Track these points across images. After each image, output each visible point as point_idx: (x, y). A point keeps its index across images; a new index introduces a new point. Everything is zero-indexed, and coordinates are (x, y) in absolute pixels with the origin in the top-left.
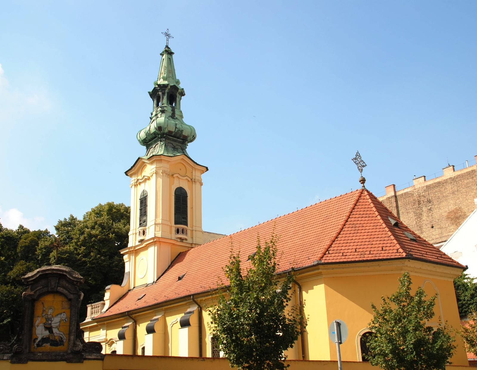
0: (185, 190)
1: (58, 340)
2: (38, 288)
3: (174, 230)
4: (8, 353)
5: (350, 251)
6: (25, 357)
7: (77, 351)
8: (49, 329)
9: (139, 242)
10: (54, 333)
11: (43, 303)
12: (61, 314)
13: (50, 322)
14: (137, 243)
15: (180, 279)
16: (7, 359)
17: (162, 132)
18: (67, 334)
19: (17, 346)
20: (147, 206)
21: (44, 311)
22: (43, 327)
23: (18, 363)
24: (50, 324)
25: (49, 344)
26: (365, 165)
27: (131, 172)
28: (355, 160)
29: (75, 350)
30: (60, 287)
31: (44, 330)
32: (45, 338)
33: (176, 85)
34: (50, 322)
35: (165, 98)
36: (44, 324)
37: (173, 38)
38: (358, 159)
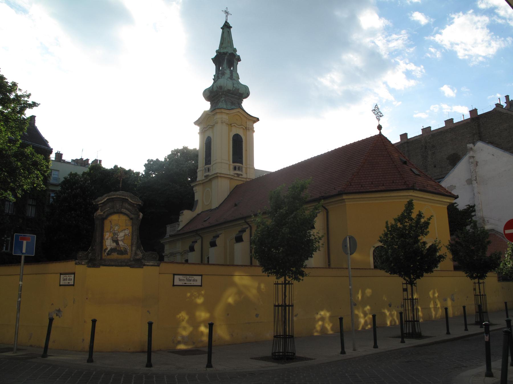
0: (241, 136)
1: (123, 250)
2: (106, 210)
3: (232, 167)
4: (85, 260)
5: (367, 183)
6: (98, 263)
7: (138, 259)
8: (116, 241)
9: (205, 177)
10: (120, 244)
11: (110, 221)
12: (125, 230)
13: (116, 236)
14: (204, 178)
15: (236, 205)
16: (85, 264)
18: (130, 246)
19: (92, 254)
21: (111, 227)
22: (111, 240)
23: (93, 267)
24: (117, 238)
25: (116, 253)
26: (382, 115)
28: (374, 111)
29: (136, 258)
30: (123, 208)
31: (112, 242)
32: (113, 249)
33: (234, 52)
34: (116, 236)
36: (112, 237)
37: (231, 15)
38: (377, 110)
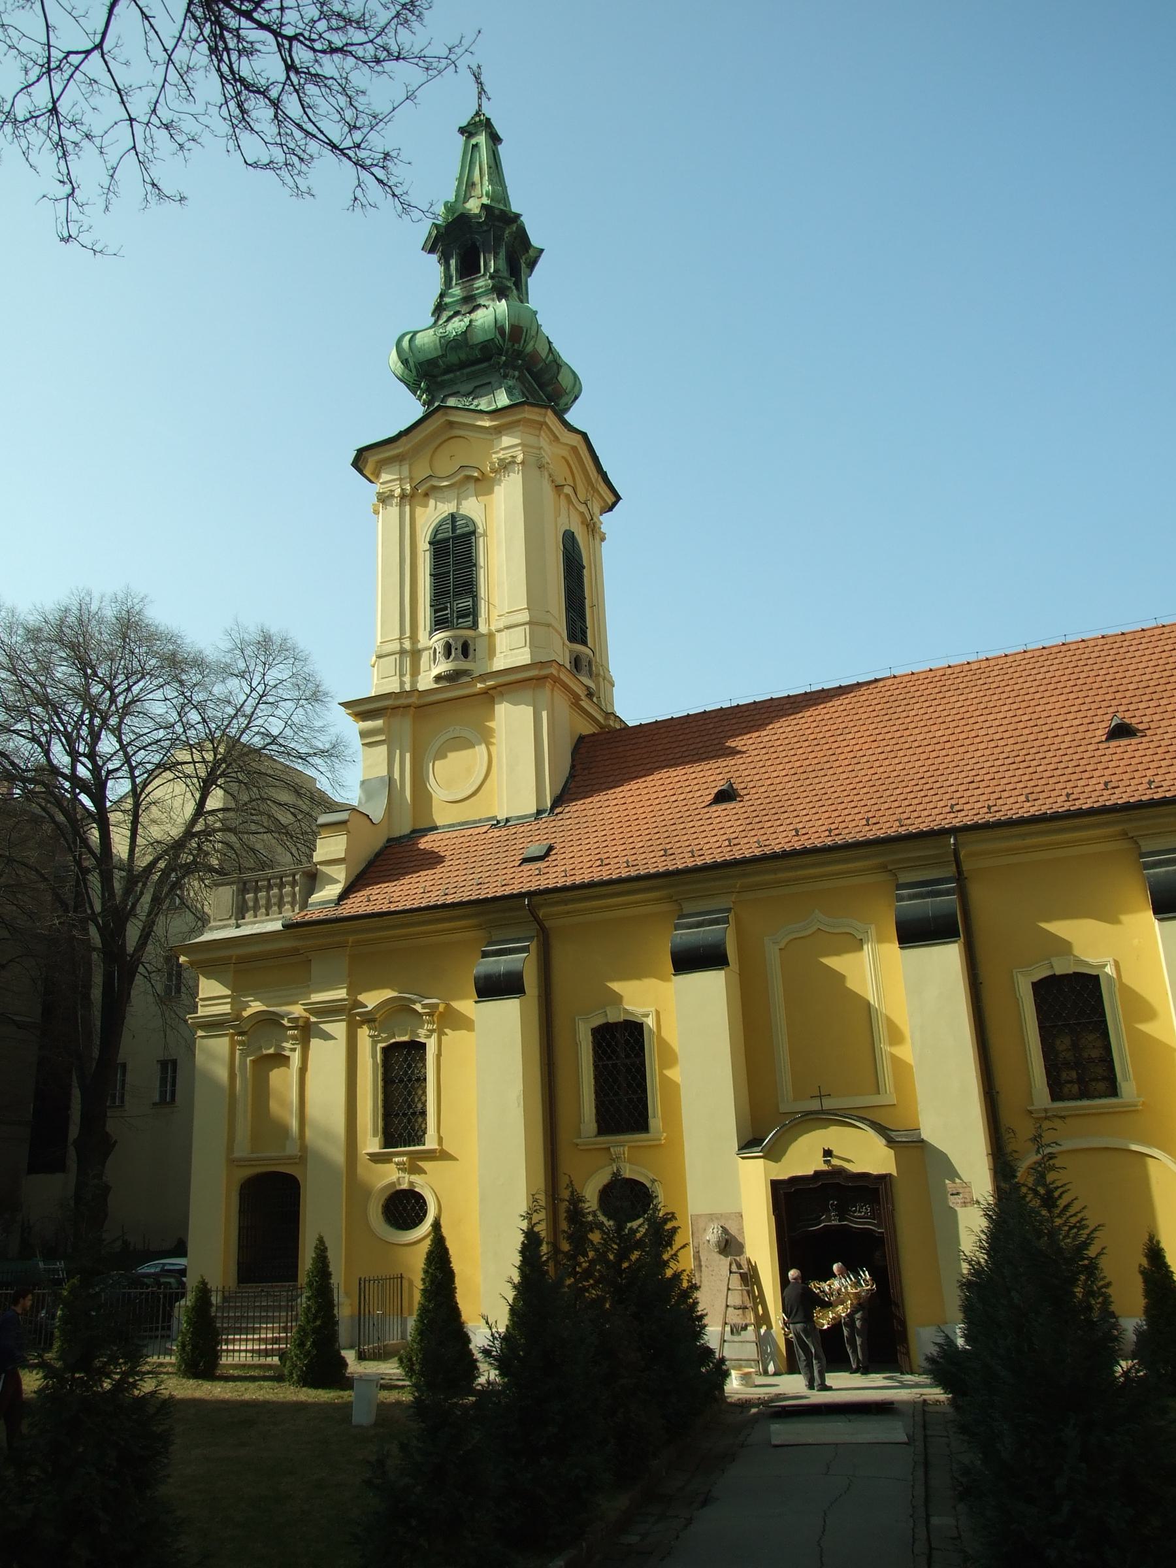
17: (516, 346)
27: (394, 449)
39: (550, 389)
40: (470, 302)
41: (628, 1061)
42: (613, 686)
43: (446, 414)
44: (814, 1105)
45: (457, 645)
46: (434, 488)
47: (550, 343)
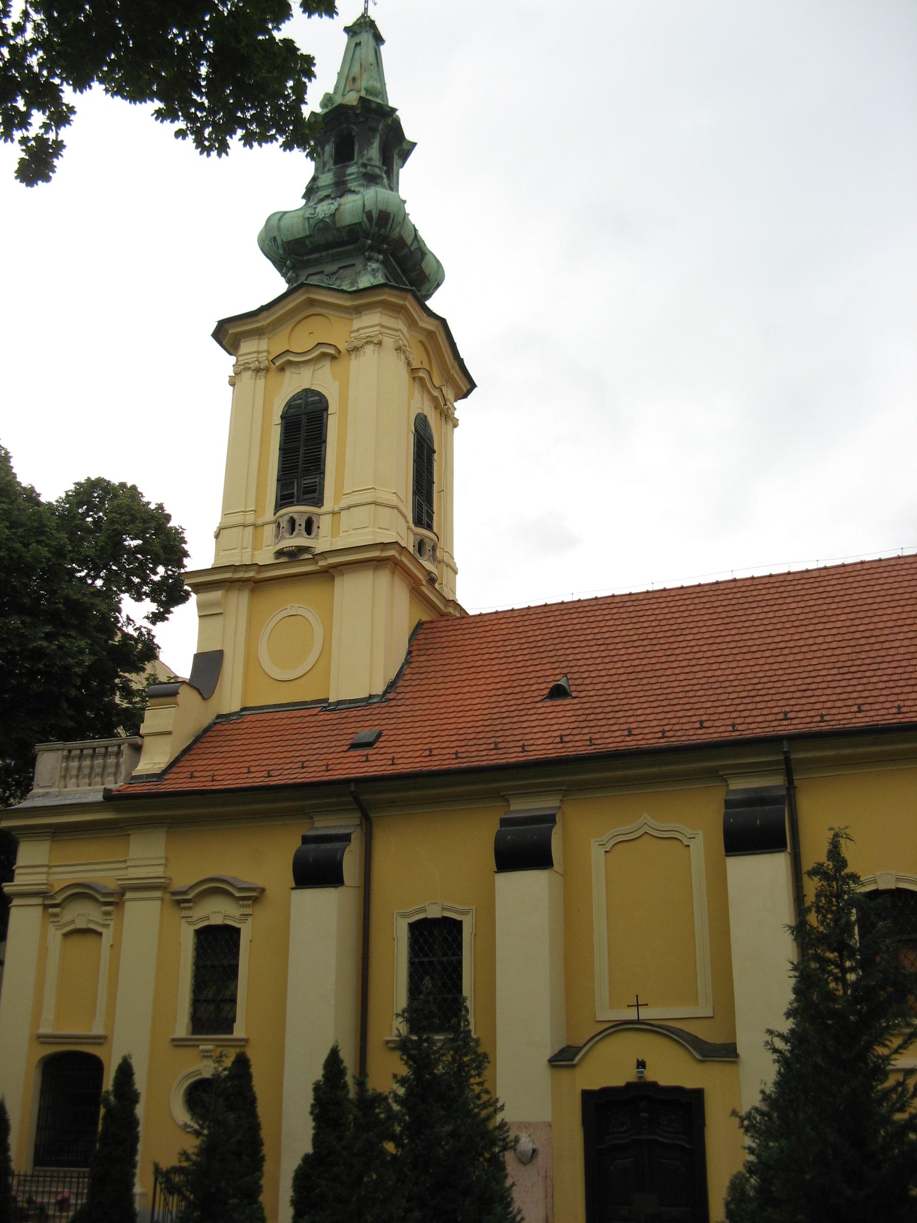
17: (382, 231)
20: (325, 442)
35: (375, 144)
39: (413, 275)
40: (341, 188)
41: (445, 959)
42: (456, 573)
43: (308, 292)
44: (631, 1015)
45: (301, 522)
46: (290, 363)
47: (416, 230)
